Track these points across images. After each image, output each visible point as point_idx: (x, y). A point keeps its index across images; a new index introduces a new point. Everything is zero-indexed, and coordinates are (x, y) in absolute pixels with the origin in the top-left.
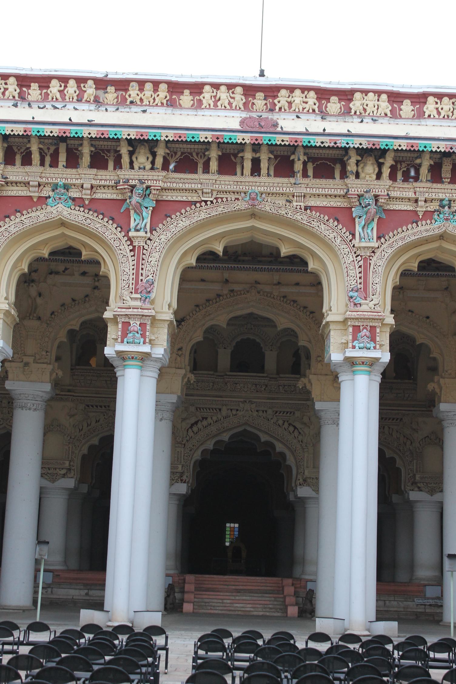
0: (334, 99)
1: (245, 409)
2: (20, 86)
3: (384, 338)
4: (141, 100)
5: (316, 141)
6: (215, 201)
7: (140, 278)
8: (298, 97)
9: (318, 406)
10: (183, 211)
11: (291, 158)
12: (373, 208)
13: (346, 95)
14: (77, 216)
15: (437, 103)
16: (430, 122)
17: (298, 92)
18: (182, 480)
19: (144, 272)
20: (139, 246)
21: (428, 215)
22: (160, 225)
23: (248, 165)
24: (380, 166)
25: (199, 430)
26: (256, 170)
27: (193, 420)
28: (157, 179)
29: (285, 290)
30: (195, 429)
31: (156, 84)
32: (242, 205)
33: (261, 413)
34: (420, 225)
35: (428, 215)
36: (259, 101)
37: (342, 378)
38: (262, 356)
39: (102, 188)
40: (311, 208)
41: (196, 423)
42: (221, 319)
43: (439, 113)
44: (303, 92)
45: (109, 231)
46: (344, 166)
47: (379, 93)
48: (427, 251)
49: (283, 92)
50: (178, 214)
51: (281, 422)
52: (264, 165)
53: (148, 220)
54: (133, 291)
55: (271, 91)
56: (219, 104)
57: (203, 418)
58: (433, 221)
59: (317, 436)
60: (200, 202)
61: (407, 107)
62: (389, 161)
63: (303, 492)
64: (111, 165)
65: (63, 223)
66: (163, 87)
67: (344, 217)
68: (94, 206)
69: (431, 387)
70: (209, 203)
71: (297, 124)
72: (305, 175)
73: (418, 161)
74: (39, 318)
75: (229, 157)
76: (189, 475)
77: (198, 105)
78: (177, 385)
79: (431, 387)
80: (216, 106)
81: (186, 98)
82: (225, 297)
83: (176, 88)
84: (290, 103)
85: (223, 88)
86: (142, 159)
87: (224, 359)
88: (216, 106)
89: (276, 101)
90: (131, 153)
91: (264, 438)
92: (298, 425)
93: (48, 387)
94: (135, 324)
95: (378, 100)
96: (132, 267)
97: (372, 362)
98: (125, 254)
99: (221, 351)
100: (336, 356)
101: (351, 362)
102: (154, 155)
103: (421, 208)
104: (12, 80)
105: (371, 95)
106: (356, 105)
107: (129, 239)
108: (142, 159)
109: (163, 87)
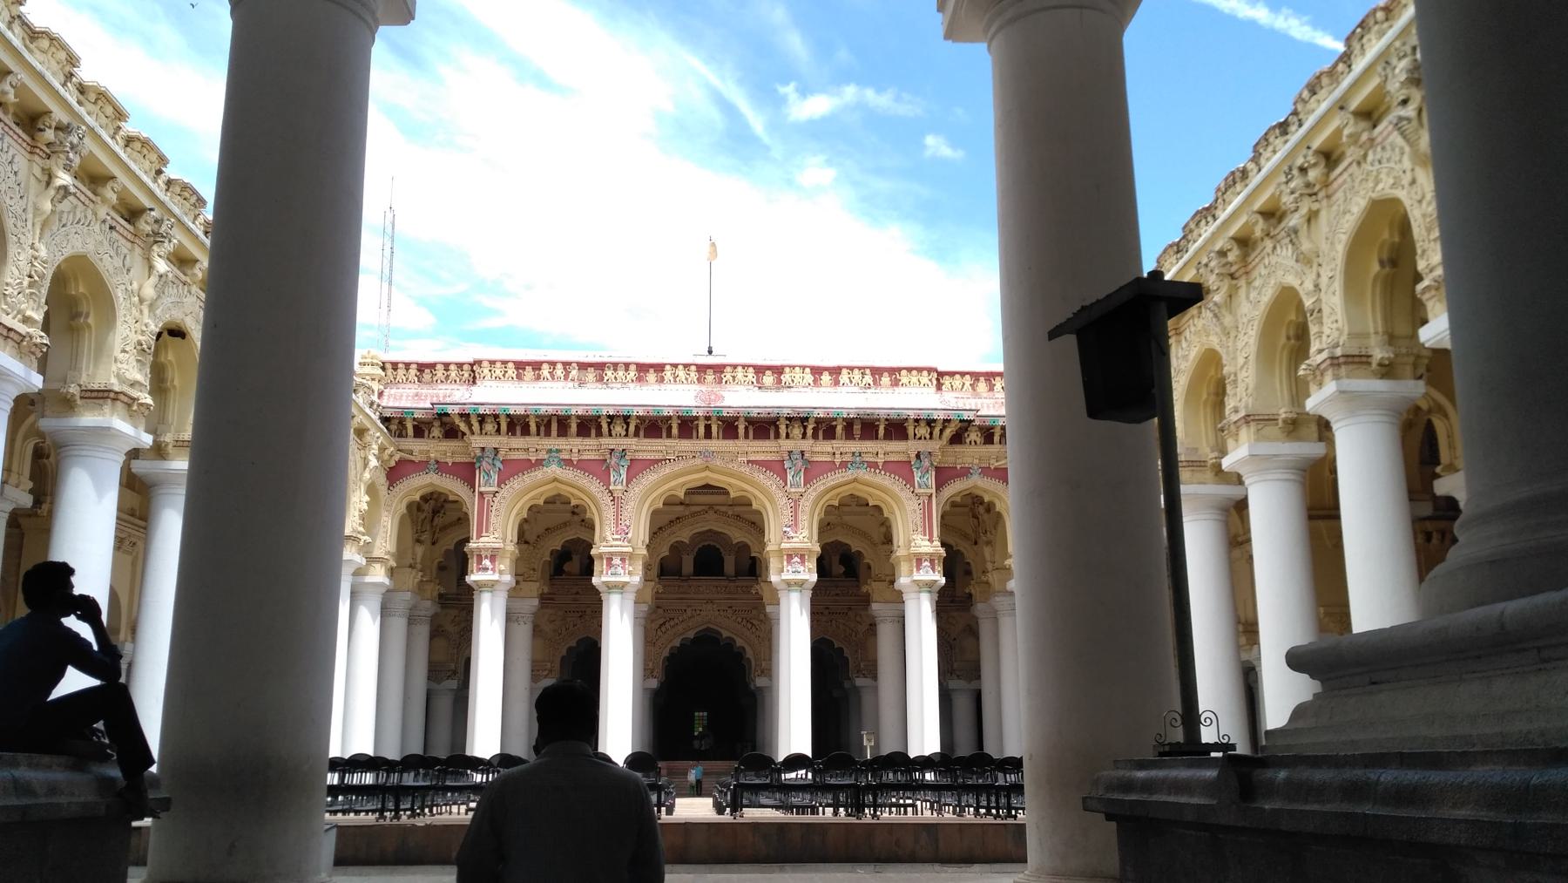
0: (768, 373)
1: (708, 609)
2: (517, 369)
3: (813, 565)
5: (754, 413)
8: (740, 372)
9: (769, 609)
12: (800, 463)
13: (778, 370)
14: (568, 474)
16: (844, 389)
21: (844, 465)
23: (702, 430)
24: (805, 428)
26: (708, 435)
28: (631, 443)
29: (738, 509)
31: (627, 366)
32: (698, 461)
35: (844, 465)
36: (710, 377)
37: (781, 595)
38: (722, 560)
40: (753, 462)
42: (684, 535)
45: (593, 486)
46: (777, 428)
47: (803, 367)
48: (846, 491)
49: (728, 369)
52: (714, 429)
53: (624, 476)
55: (719, 369)
59: (770, 631)
61: (826, 377)
62: (810, 427)
63: (760, 682)
64: (593, 432)
65: (555, 480)
66: (633, 367)
67: (777, 468)
68: (583, 466)
69: (864, 589)
71: (741, 398)
72: (747, 437)
75: (687, 425)
76: (659, 671)
77: (661, 380)
78: (648, 596)
79: (864, 589)
81: (651, 376)
83: (643, 368)
86: (618, 429)
87: (688, 566)
91: (725, 634)
93: (536, 602)
94: (617, 561)
97: (800, 584)
99: (685, 557)
100: (774, 578)
101: (789, 584)
102: (628, 424)
103: (838, 460)
104: (511, 365)
106: (786, 378)
108: (618, 429)
109: (633, 367)
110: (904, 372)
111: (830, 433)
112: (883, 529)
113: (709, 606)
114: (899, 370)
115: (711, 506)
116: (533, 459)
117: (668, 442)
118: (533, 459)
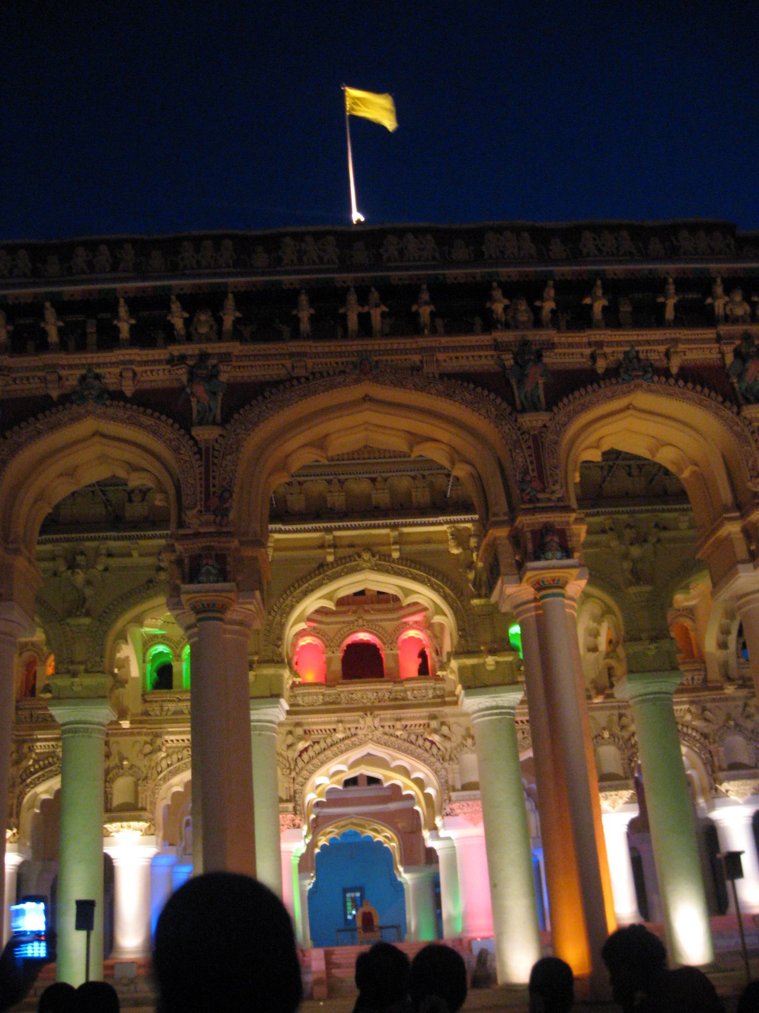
4: (198, 263)
6: (311, 377)
7: (212, 489)
10: (267, 394)
11: (414, 308)
15: (595, 239)
17: (410, 236)
18: (294, 825)
19: (216, 482)
20: (207, 449)
21: (613, 373)
22: (236, 416)
23: (353, 322)
25: (311, 758)
27: (301, 745)
30: (305, 756)
33: (387, 729)
34: (603, 386)
39: (149, 373)
41: (306, 749)
43: (600, 250)
44: (416, 237)
50: (260, 398)
51: (413, 738)
54: (203, 509)
56: (305, 259)
57: (314, 743)
58: (620, 380)
60: (291, 379)
70: (303, 380)
72: (434, 331)
73: (588, 301)
74: (88, 614)
80: (300, 261)
82: (330, 566)
84: (401, 252)
85: (309, 239)
88: (300, 261)
89: (382, 251)
90: (187, 322)
92: (436, 738)
95: (518, 240)
96: (198, 476)
98: (187, 458)
103: (601, 365)
105: (508, 234)
107: (192, 438)
110: (684, 234)
111: (581, 320)
112: (627, 565)
113: (369, 719)
114: (675, 228)
115: (368, 548)
116: (55, 394)
117: (294, 346)
118: (55, 394)
